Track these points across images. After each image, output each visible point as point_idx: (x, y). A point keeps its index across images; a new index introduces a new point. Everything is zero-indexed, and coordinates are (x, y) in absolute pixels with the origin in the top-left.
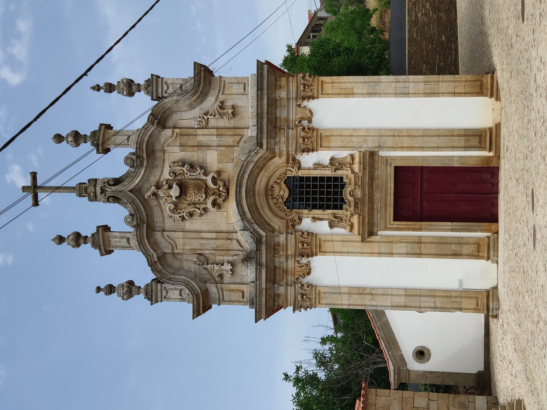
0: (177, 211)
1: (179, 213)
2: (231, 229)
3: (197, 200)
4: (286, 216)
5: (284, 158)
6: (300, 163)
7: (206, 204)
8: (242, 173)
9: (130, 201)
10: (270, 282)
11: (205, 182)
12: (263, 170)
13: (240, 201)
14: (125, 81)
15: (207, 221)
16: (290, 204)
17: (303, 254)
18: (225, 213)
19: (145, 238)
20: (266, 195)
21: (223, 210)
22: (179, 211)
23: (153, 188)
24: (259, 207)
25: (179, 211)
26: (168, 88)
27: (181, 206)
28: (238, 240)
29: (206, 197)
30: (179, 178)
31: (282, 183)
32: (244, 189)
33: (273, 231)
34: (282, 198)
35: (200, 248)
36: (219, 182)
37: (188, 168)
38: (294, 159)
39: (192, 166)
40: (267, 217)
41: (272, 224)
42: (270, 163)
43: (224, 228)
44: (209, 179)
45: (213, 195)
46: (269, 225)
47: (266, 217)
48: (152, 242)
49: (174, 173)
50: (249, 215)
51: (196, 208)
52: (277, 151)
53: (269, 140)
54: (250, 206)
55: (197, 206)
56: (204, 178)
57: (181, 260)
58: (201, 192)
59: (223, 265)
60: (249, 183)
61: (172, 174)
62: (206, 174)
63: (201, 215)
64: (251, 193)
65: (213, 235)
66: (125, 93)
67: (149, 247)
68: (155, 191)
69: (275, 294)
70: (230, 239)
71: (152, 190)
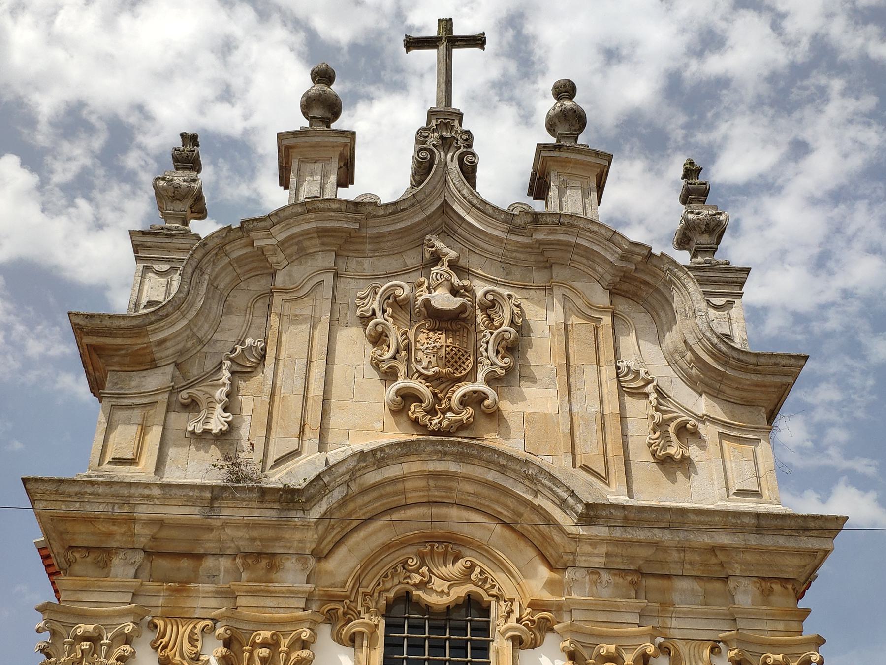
0: (389, 305)
1: (384, 311)
2: (331, 439)
3: (420, 355)
4: (365, 594)
5: (546, 596)
6: (534, 645)
7: (407, 376)
8: (503, 461)
9: (419, 198)
10: (154, 538)
11: (471, 376)
12: (507, 533)
13: (418, 453)
14: (722, 218)
15: (359, 380)
16: (403, 611)
17: (236, 646)
19: (320, 224)
20: (431, 539)
21: (390, 419)
22: (389, 310)
23: (453, 254)
24: (395, 516)
25: (389, 310)
26: (716, 308)
27: (403, 317)
28: (295, 453)
29: (427, 378)
30: (479, 320)
31: (469, 587)
32: (452, 467)
33: (320, 556)
34: (423, 585)
35: (283, 355)
36: (470, 410)
37: (507, 335)
38: (545, 627)
39: (514, 347)
40: (365, 539)
41: (342, 551)
42: (530, 553)
43: (336, 419)
44: (480, 385)
45: (435, 395)
46: (337, 544)
47: (362, 533)
48: (307, 243)
49: (493, 304)
50: (373, 477)
51: (397, 351)
52: (568, 575)
53: (603, 549)
54: (400, 486)
55: (403, 353)
56: (481, 376)
57: (250, 309)
58: (442, 363)
59: (226, 410)
60: (468, 487)
61: (490, 297)
62: (492, 380)
63: (376, 364)
64: (440, 492)
65: (316, 390)
66: (690, 216)
67: (296, 230)
68: (446, 260)
69: (109, 552)
70: (302, 432)
71: (447, 250)
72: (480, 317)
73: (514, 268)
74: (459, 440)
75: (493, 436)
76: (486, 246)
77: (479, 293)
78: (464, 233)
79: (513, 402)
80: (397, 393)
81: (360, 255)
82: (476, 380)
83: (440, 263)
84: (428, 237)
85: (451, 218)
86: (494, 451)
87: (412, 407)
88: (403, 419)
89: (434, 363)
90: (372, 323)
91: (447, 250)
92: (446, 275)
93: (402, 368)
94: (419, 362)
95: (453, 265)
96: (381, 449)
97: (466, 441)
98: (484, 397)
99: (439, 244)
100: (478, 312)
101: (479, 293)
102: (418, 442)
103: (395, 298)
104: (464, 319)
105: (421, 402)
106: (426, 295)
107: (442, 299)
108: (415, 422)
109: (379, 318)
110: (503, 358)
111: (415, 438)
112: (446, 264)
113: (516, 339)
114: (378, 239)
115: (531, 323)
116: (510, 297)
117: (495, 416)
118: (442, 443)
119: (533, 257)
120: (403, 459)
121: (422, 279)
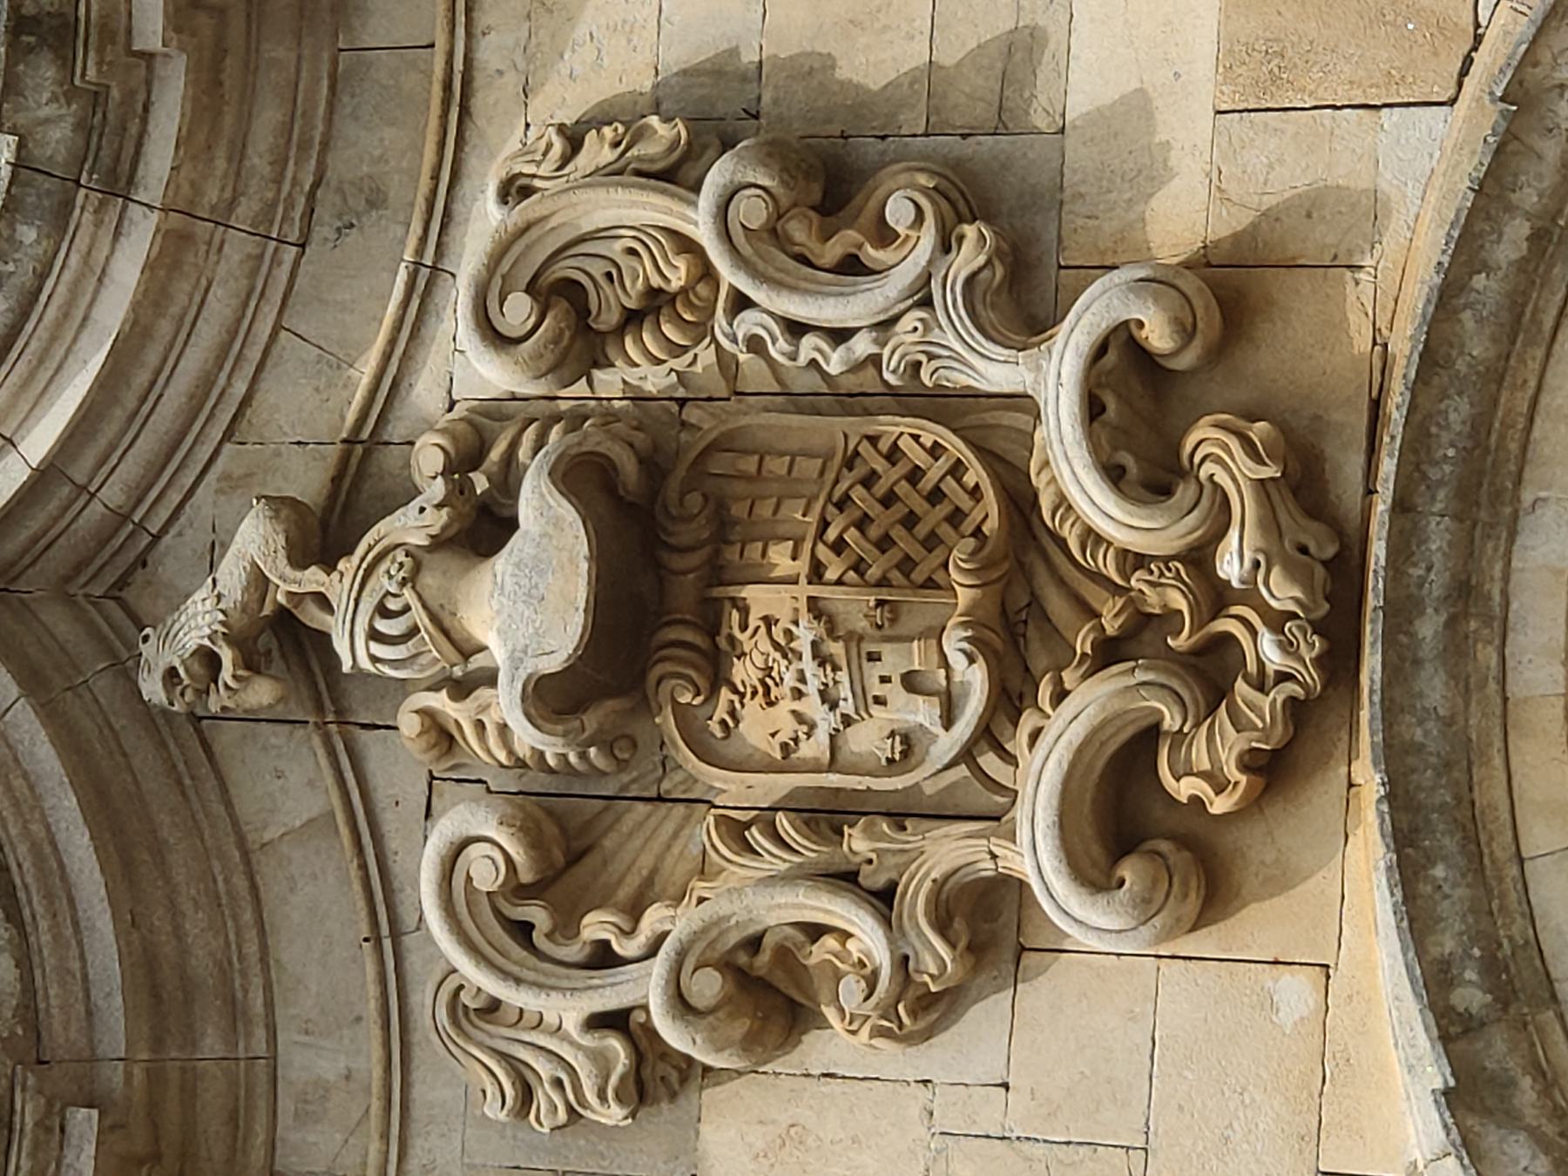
0: (567, 926)
1: (603, 958)
3: (868, 739)
7: (995, 817)
11: (996, 431)
15: (1018, 1114)
18: (1295, 990)
21: (1255, 927)
23: (255, 539)
25: (597, 926)
29: (1010, 699)
30: (655, 380)
36: (1206, 440)
37: (751, 211)
44: (1053, 375)
45: (1108, 653)
49: (561, 294)
51: (845, 879)
55: (858, 842)
56: (995, 371)
58: (920, 608)
61: (517, 311)
62: (1020, 303)
63: (921, 1009)
68: (288, 582)
71: (231, 575)
72: (639, 371)
73: (341, 165)
74: (1382, 506)
75: (1359, 294)
76: (208, 334)
77: (490, 375)
78: (130, 468)
79: (1151, 173)
80: (1095, 877)
81: (262, 1105)
82: (1022, 402)
83: (312, 616)
84: (152, 688)
85: (39, 547)
86: (1449, 296)
87: (1184, 789)
88: (1256, 846)
89: (916, 656)
90: (673, 1035)
91: (231, 575)
92: (382, 582)
93: (948, 851)
94: (908, 746)
95: (324, 533)
96: (1435, 983)
97: (1388, 466)
98: (1120, 350)
99: (197, 621)
100: (609, 382)
101: (490, 375)
102: (1393, 757)
103: (518, 891)
104: (654, 465)
105: (1150, 735)
106: (505, 703)
107: (531, 602)
108: (1275, 770)
109: (645, 986)
110: (885, 235)
111: (1370, 780)
112: (313, 578)
113: (777, 153)
114: (159, 989)
115: (677, 55)
116: (514, 190)
117: (1232, 287)
118: (1400, 614)
119: (278, 51)
120: (1501, 848)
121: (409, 724)
